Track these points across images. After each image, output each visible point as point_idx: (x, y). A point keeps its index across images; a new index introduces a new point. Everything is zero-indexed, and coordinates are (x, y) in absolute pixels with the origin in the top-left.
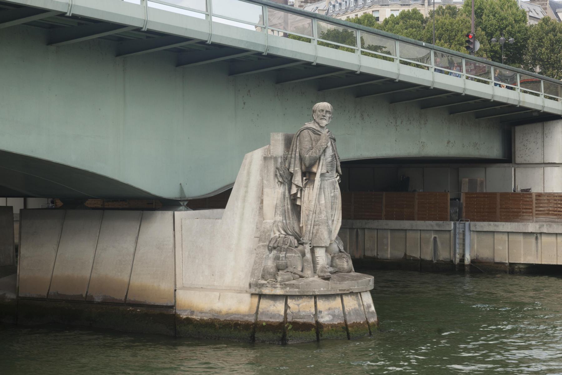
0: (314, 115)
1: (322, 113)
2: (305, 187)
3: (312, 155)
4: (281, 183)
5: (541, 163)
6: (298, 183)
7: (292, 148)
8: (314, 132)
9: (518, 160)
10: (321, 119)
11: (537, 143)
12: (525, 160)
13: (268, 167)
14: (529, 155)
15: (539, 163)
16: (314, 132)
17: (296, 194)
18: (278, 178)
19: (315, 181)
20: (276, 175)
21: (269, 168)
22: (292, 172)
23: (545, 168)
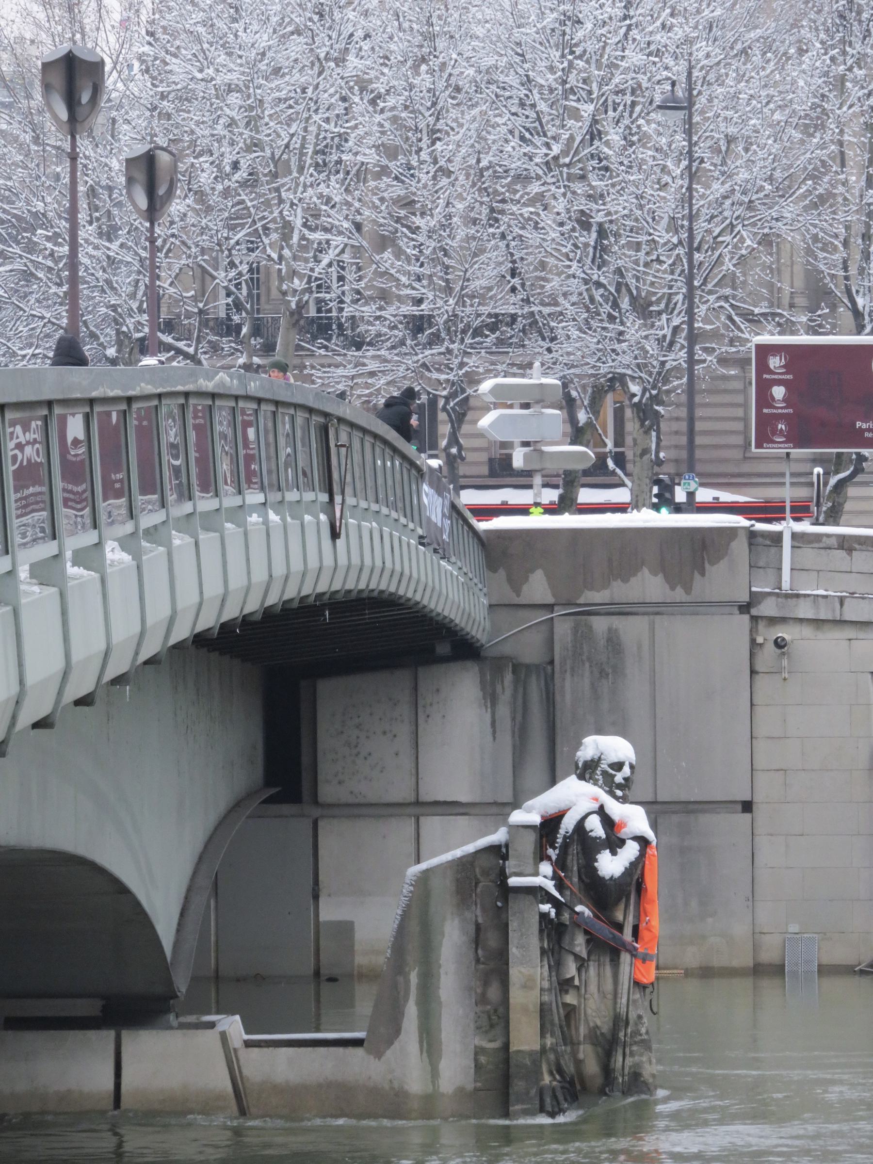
2: (589, 960)
4: (543, 952)
5: (408, 801)
6: (581, 951)
9: (328, 792)
11: (395, 736)
12: (352, 793)
14: (366, 778)
15: (401, 801)
17: (573, 978)
18: (541, 940)
20: (541, 931)
22: (568, 923)
23: (422, 819)
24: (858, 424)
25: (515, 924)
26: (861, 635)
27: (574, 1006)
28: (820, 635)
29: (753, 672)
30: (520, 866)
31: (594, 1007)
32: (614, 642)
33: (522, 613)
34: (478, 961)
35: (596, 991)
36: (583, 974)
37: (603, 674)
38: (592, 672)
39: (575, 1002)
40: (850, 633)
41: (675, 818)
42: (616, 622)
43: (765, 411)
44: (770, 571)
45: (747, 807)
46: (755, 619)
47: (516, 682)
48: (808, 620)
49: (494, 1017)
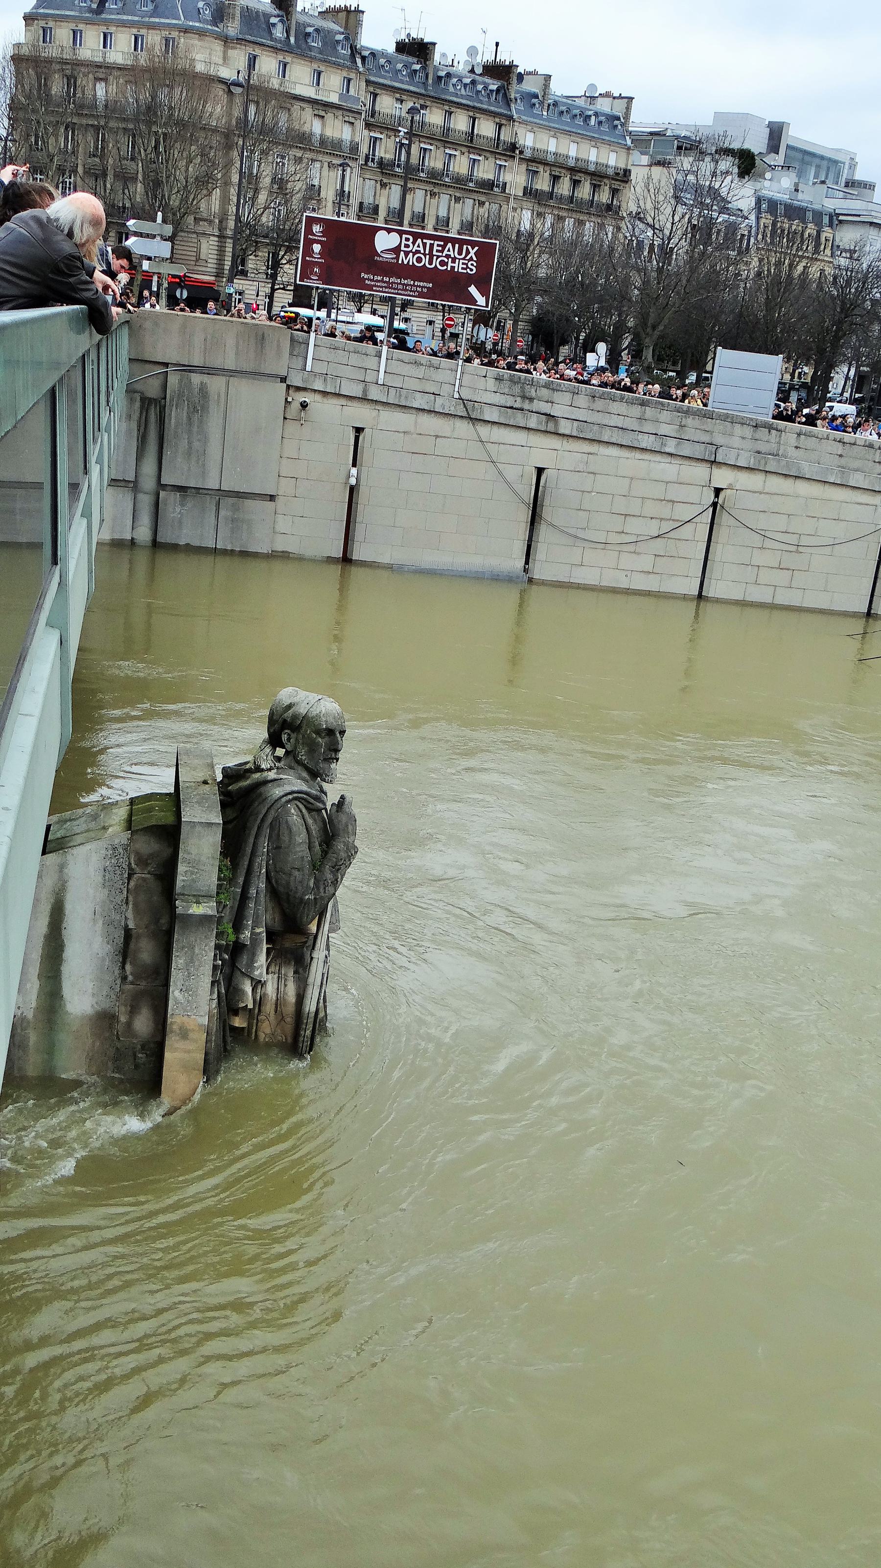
0: (284, 737)
1: (327, 739)
3: (325, 892)
6: (261, 974)
7: (246, 863)
8: (310, 806)
10: (325, 760)
13: (192, 948)
16: (310, 806)
18: (214, 974)
19: (315, 961)
20: (215, 967)
21: (197, 951)
24: (363, 275)
25: (181, 961)
26: (349, 403)
27: (243, 1028)
28: (325, 400)
29: (285, 418)
30: (192, 874)
31: (268, 1031)
32: (203, 391)
33: (148, 366)
34: (124, 978)
35: (273, 1012)
36: (259, 991)
37: (195, 410)
38: (188, 408)
39: (245, 1025)
40: (343, 401)
41: (231, 500)
42: (206, 378)
43: (307, 258)
44: (300, 359)
45: (272, 498)
46: (288, 387)
47: (142, 407)
48: (320, 391)
49: (140, 1055)
